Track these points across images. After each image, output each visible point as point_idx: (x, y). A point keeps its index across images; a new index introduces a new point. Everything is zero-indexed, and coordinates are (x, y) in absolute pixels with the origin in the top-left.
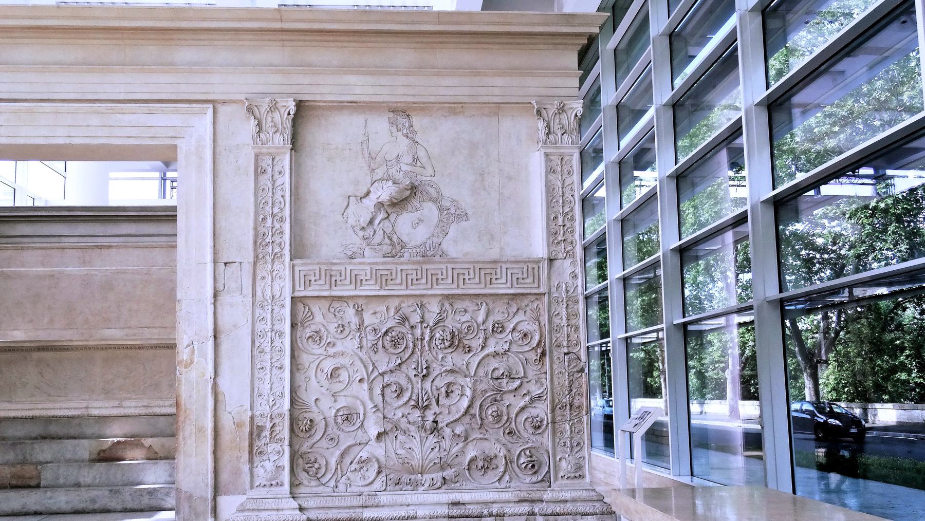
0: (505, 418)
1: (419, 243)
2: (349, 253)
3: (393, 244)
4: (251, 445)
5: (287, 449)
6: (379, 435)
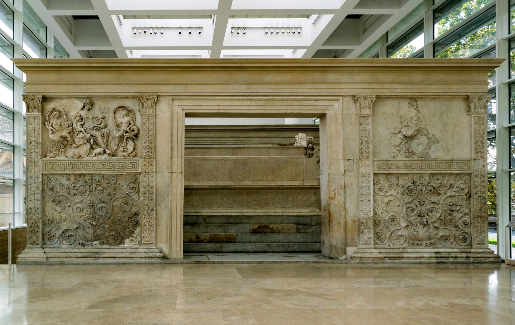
0: (454, 221)
1: (419, 152)
2: (392, 156)
3: (409, 153)
4: (359, 229)
5: (372, 231)
6: (406, 226)
